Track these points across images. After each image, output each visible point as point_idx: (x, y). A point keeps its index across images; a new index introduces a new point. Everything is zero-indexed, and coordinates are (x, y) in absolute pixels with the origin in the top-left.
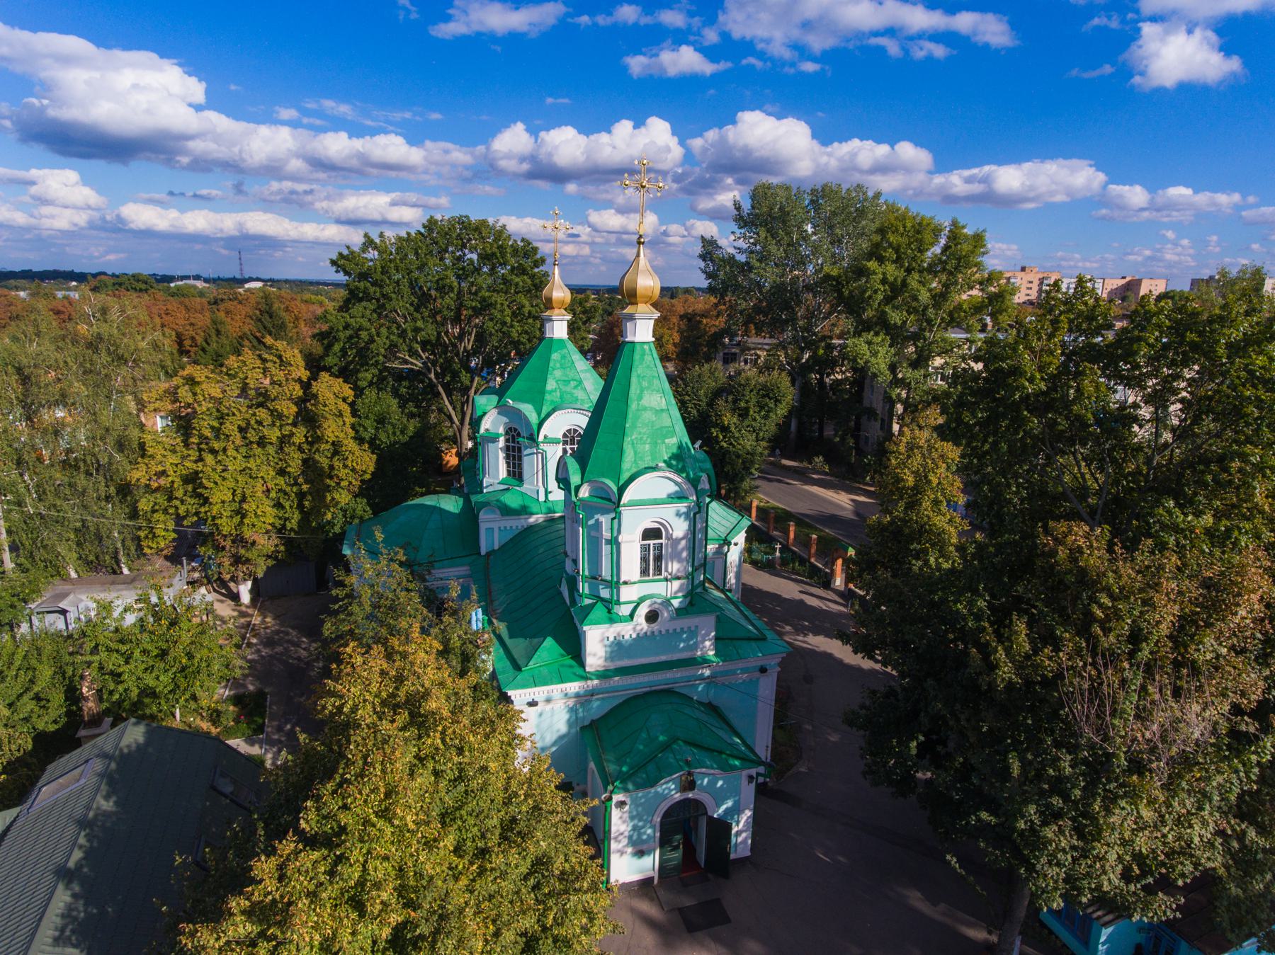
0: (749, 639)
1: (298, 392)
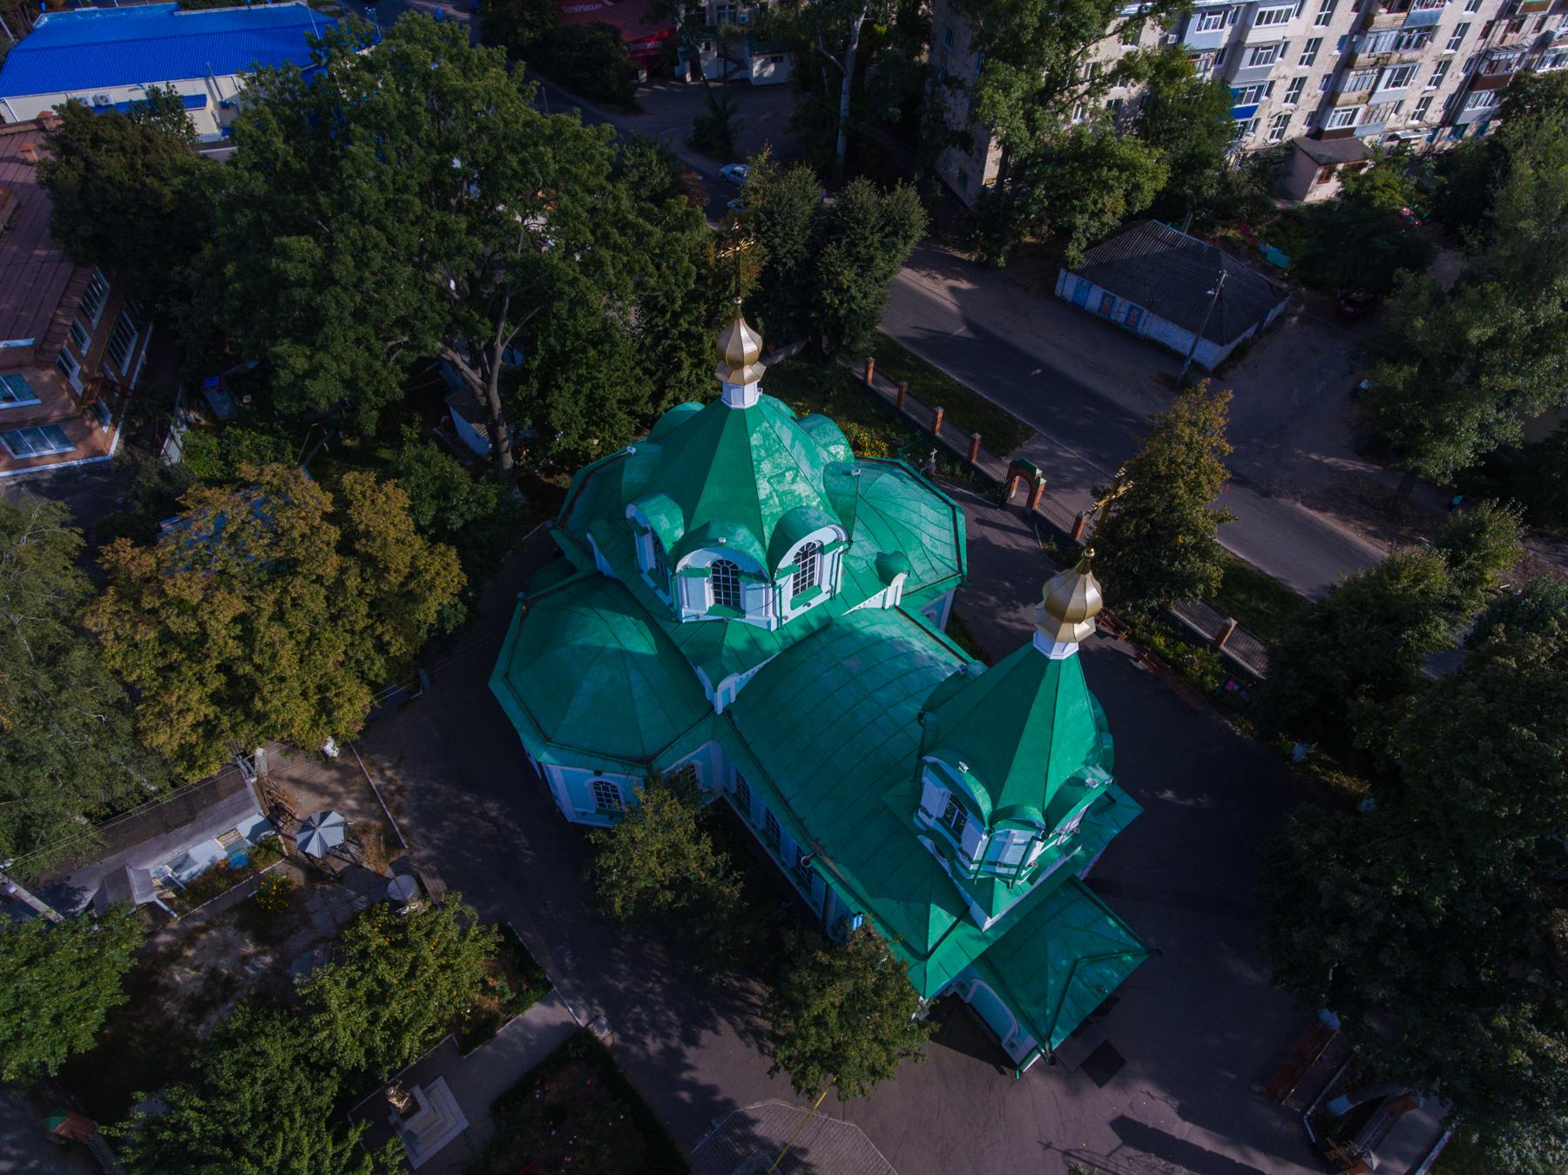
1: (334, 534)
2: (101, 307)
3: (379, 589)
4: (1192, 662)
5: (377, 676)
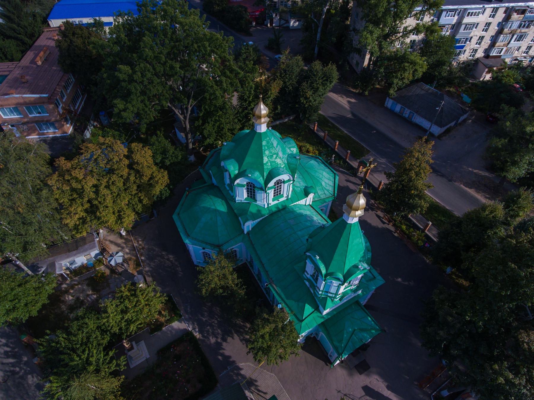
0: (371, 280)
1: (127, 162)
2: (71, 87)
3: (141, 182)
4: (414, 235)
5: (138, 210)
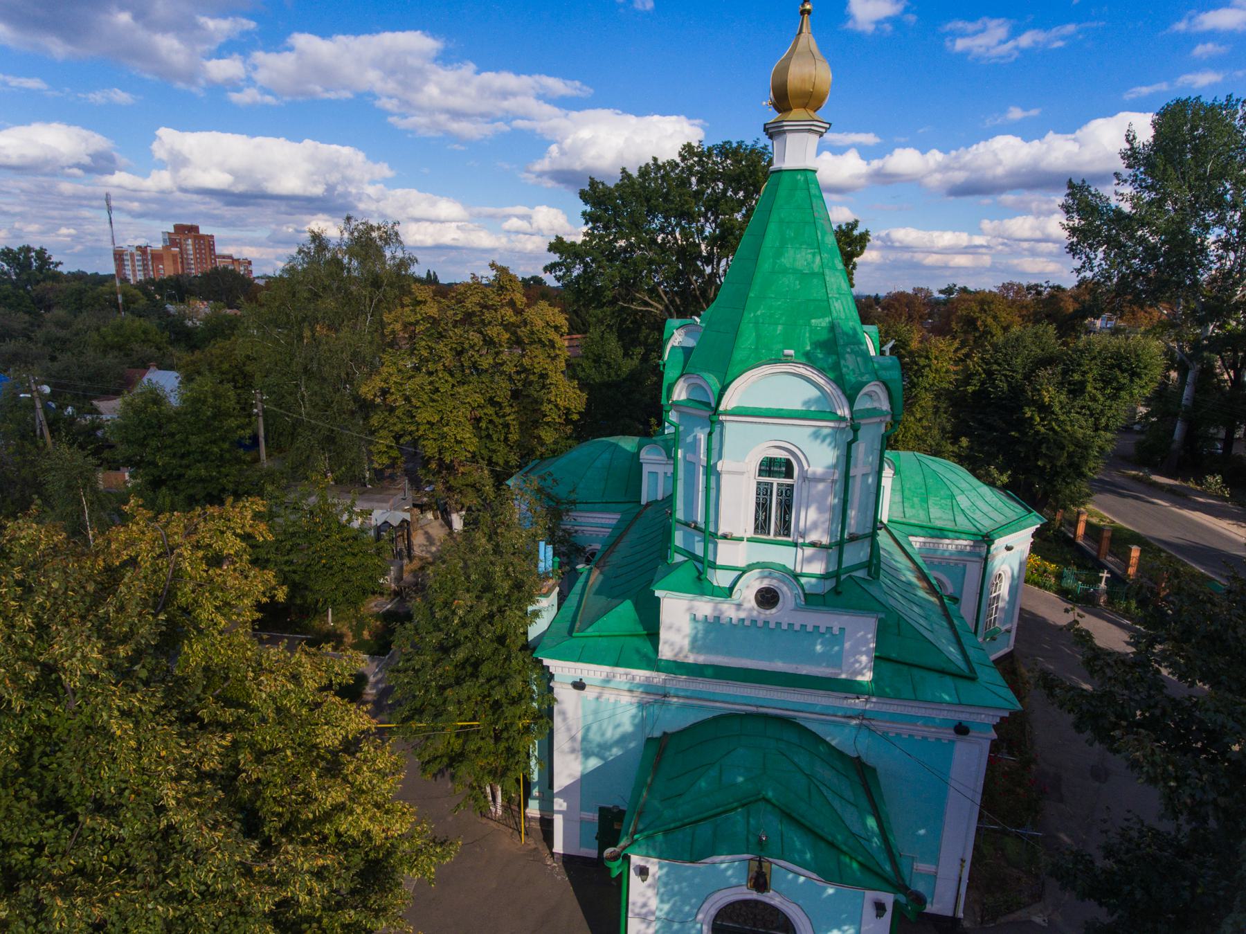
0: (943, 672)
